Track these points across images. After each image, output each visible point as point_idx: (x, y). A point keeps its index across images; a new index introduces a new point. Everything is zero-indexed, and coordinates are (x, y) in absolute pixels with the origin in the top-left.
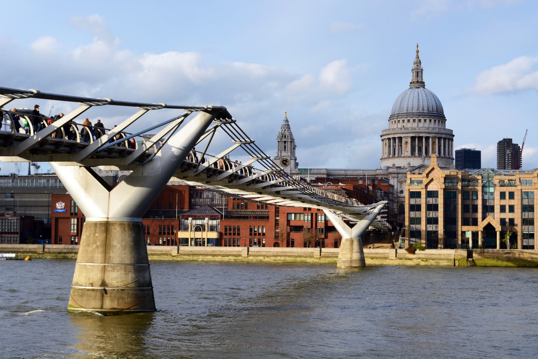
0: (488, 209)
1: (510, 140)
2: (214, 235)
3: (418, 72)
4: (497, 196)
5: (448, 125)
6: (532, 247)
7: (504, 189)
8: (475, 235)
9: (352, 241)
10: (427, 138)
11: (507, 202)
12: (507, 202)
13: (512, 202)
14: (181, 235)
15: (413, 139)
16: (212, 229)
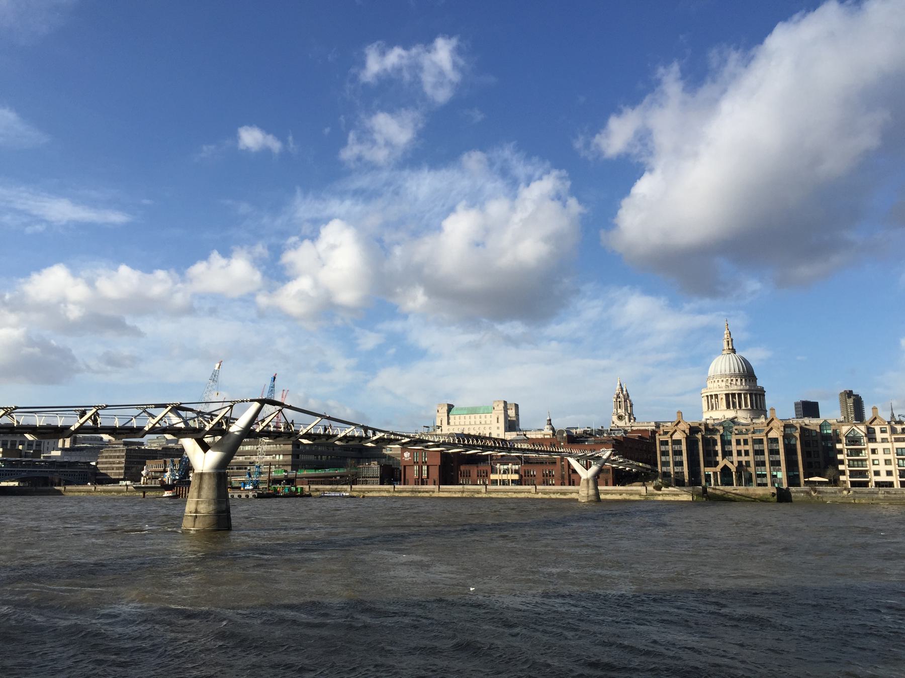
0: (727, 454)
1: (851, 392)
2: (516, 477)
3: (731, 341)
4: (734, 443)
5: (760, 383)
6: (766, 485)
7: (739, 437)
8: (715, 473)
9: (588, 481)
10: (740, 395)
11: (742, 448)
12: (742, 448)
13: (747, 447)
14: (493, 477)
15: (727, 395)
16: (516, 472)
